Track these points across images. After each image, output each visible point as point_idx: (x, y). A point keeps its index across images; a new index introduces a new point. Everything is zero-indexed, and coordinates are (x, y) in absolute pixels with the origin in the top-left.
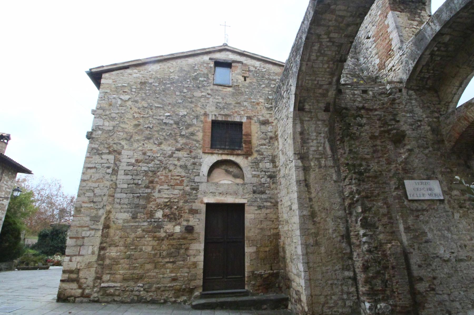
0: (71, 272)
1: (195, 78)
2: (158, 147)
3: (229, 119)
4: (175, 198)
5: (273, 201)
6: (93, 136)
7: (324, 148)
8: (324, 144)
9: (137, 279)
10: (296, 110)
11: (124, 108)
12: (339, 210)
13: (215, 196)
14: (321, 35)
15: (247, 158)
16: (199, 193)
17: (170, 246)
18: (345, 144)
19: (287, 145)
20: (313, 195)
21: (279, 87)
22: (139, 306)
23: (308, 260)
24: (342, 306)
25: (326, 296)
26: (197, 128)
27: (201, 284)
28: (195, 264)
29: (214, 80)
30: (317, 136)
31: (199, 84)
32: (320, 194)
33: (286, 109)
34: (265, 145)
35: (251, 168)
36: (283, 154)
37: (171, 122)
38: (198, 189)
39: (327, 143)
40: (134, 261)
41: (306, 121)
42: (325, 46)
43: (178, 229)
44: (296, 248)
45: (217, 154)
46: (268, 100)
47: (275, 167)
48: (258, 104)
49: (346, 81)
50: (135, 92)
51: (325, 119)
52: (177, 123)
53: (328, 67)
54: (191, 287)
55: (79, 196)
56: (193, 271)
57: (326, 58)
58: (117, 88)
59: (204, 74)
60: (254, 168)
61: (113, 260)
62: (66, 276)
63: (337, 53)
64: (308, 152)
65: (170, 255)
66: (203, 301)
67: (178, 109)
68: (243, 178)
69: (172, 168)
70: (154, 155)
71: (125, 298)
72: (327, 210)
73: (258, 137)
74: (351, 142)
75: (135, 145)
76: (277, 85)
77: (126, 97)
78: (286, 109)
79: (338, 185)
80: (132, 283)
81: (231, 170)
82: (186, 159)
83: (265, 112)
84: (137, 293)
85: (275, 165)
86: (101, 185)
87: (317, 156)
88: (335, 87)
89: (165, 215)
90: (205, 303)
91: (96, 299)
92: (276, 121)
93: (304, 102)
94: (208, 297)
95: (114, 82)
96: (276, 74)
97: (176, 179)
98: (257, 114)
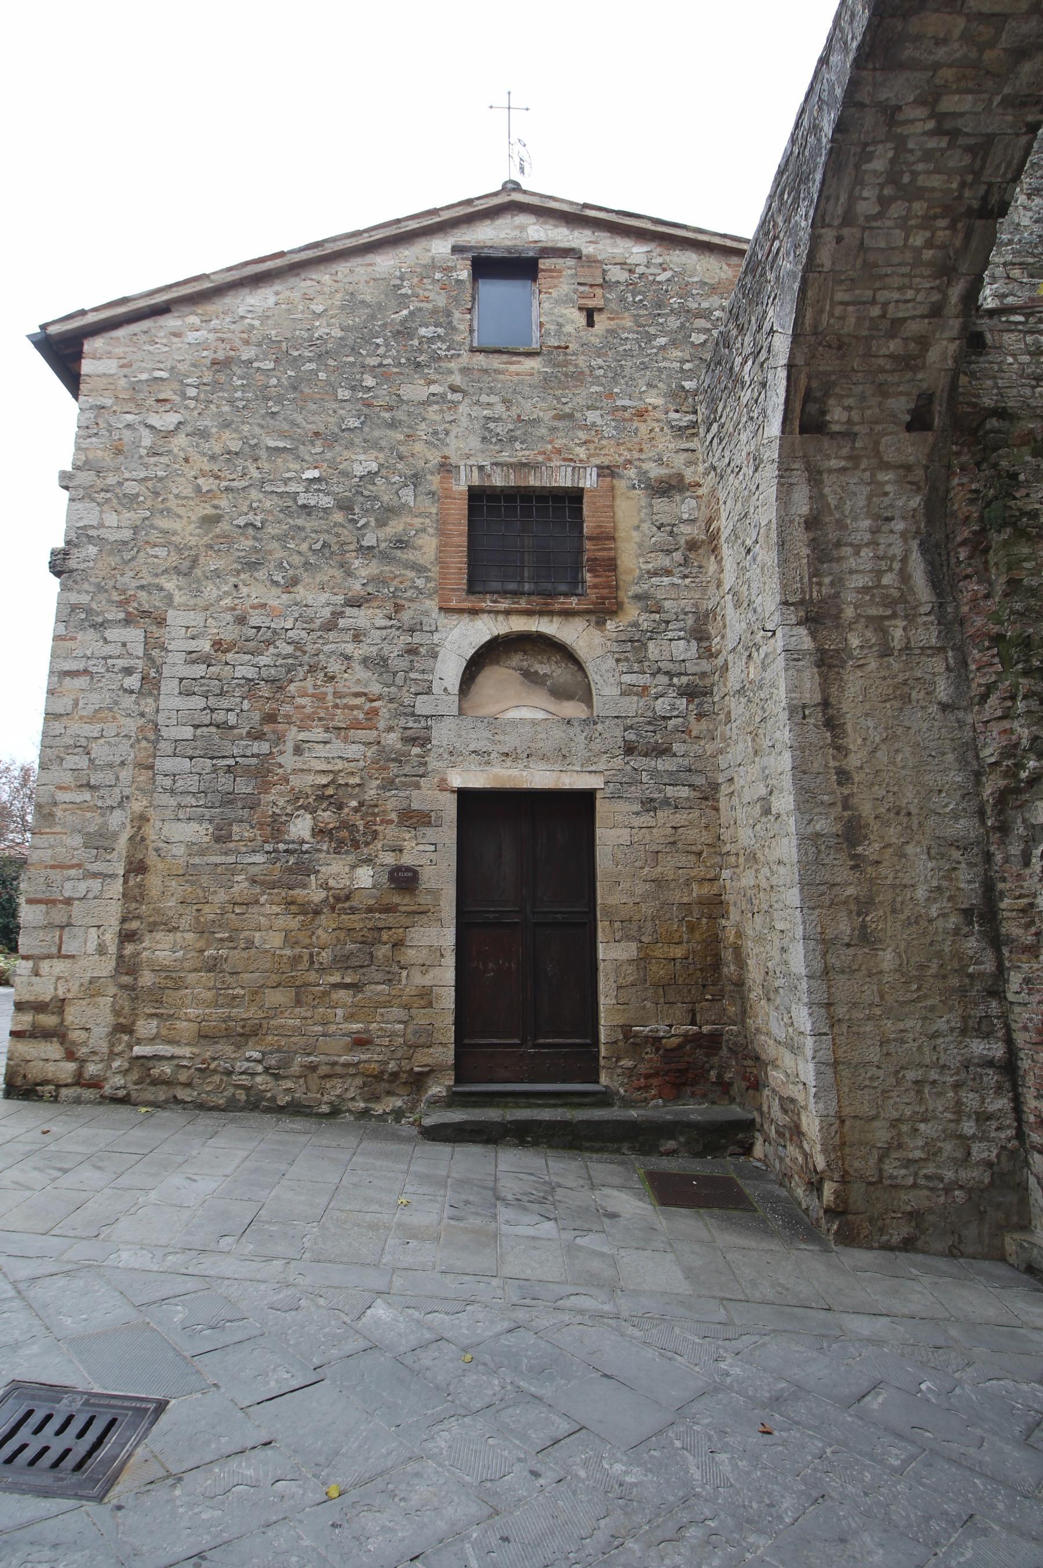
0: (39, 1007)
1: (404, 332)
2: (285, 596)
3: (533, 481)
5: (699, 780)
6: (72, 564)
7: (905, 577)
8: (904, 560)
9: (241, 1035)
10: (791, 433)
11: (164, 460)
12: (955, 816)
13: (488, 763)
14: (899, 108)
15: (600, 624)
16: (432, 754)
18: (992, 558)
19: (754, 573)
20: (854, 761)
21: (725, 341)
22: (254, 1119)
23: (830, 994)
25: (895, 1123)
26: (417, 522)
27: (451, 1060)
28: (426, 996)
29: (471, 331)
30: (875, 531)
31: (421, 351)
32: (882, 756)
33: (752, 427)
34: (668, 573)
35: (618, 660)
36: (737, 605)
37: (326, 501)
38: (429, 740)
39: (916, 557)
40: (229, 979)
41: (830, 471)
42: (919, 154)
43: (364, 877)
44: (784, 950)
45: (489, 612)
46: (678, 396)
47: (709, 654)
48: (641, 414)
49: (1004, 296)
50: (196, 399)
51: (912, 459)
52: (345, 506)
53: (929, 244)
54: (417, 1069)
55: (43, 767)
56: (422, 1018)
57: (919, 207)
58: (134, 388)
59: (434, 312)
60: (627, 659)
61: (164, 975)
62: (27, 1020)
63: (969, 178)
64: (837, 595)
65: (342, 962)
66: (456, 1116)
67: (346, 454)
68: (587, 697)
69: (335, 666)
70: (273, 625)
71: (207, 1093)
72: (909, 814)
73: (640, 545)
74: (1015, 550)
75: (210, 591)
76: (715, 333)
77: (168, 420)
78: (752, 427)
79: (958, 721)
80: (226, 1049)
81: (542, 669)
82: (384, 632)
83: (666, 443)
84: (245, 1080)
85: (708, 649)
86: (111, 730)
87: (873, 611)
88: (954, 325)
89: (321, 831)
90: (466, 1122)
91: (121, 1093)
92: (711, 479)
93: (826, 395)
94: (475, 1105)
95: (121, 367)
96: (714, 289)
97: (352, 708)
98: (636, 455)
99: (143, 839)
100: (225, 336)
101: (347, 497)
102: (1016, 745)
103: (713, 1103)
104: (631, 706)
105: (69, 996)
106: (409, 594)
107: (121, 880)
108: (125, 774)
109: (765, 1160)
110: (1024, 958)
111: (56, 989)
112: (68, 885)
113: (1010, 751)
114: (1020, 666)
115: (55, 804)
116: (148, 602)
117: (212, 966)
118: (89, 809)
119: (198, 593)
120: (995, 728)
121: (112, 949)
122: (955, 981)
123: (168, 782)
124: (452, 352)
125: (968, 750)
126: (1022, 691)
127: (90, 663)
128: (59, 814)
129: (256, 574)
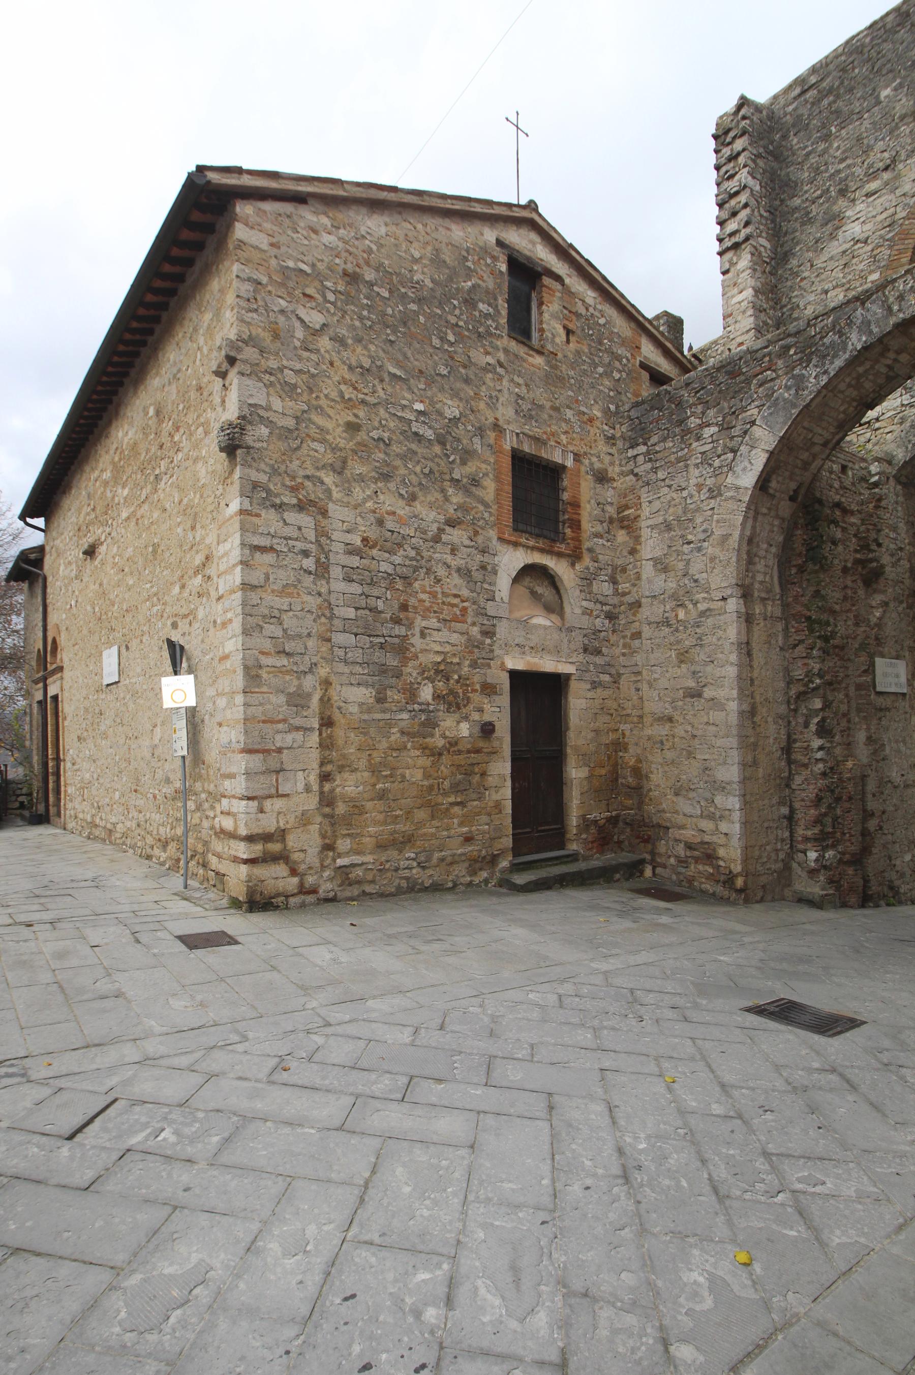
0: (267, 838)
4: (454, 655)
9: (402, 843)
13: (524, 653)
17: (454, 769)
38: (494, 634)
40: (392, 804)
43: (464, 729)
45: (524, 546)
65: (456, 788)
69: (441, 572)
71: (384, 885)
80: (393, 853)
81: (540, 590)
82: (469, 550)
84: (407, 873)
89: (438, 696)
91: (331, 894)
97: (453, 605)
99: (329, 699)
100: (351, 249)
101: (442, 434)
104: (585, 622)
105: (288, 826)
106: (480, 523)
107: (317, 733)
108: (311, 643)
111: (278, 822)
112: (278, 737)
115: (260, 667)
116: (314, 492)
117: (382, 796)
118: (288, 672)
119: (349, 492)
121: (316, 787)
123: (341, 653)
124: (498, 332)
127: (275, 541)
128: (265, 676)
129: (389, 485)
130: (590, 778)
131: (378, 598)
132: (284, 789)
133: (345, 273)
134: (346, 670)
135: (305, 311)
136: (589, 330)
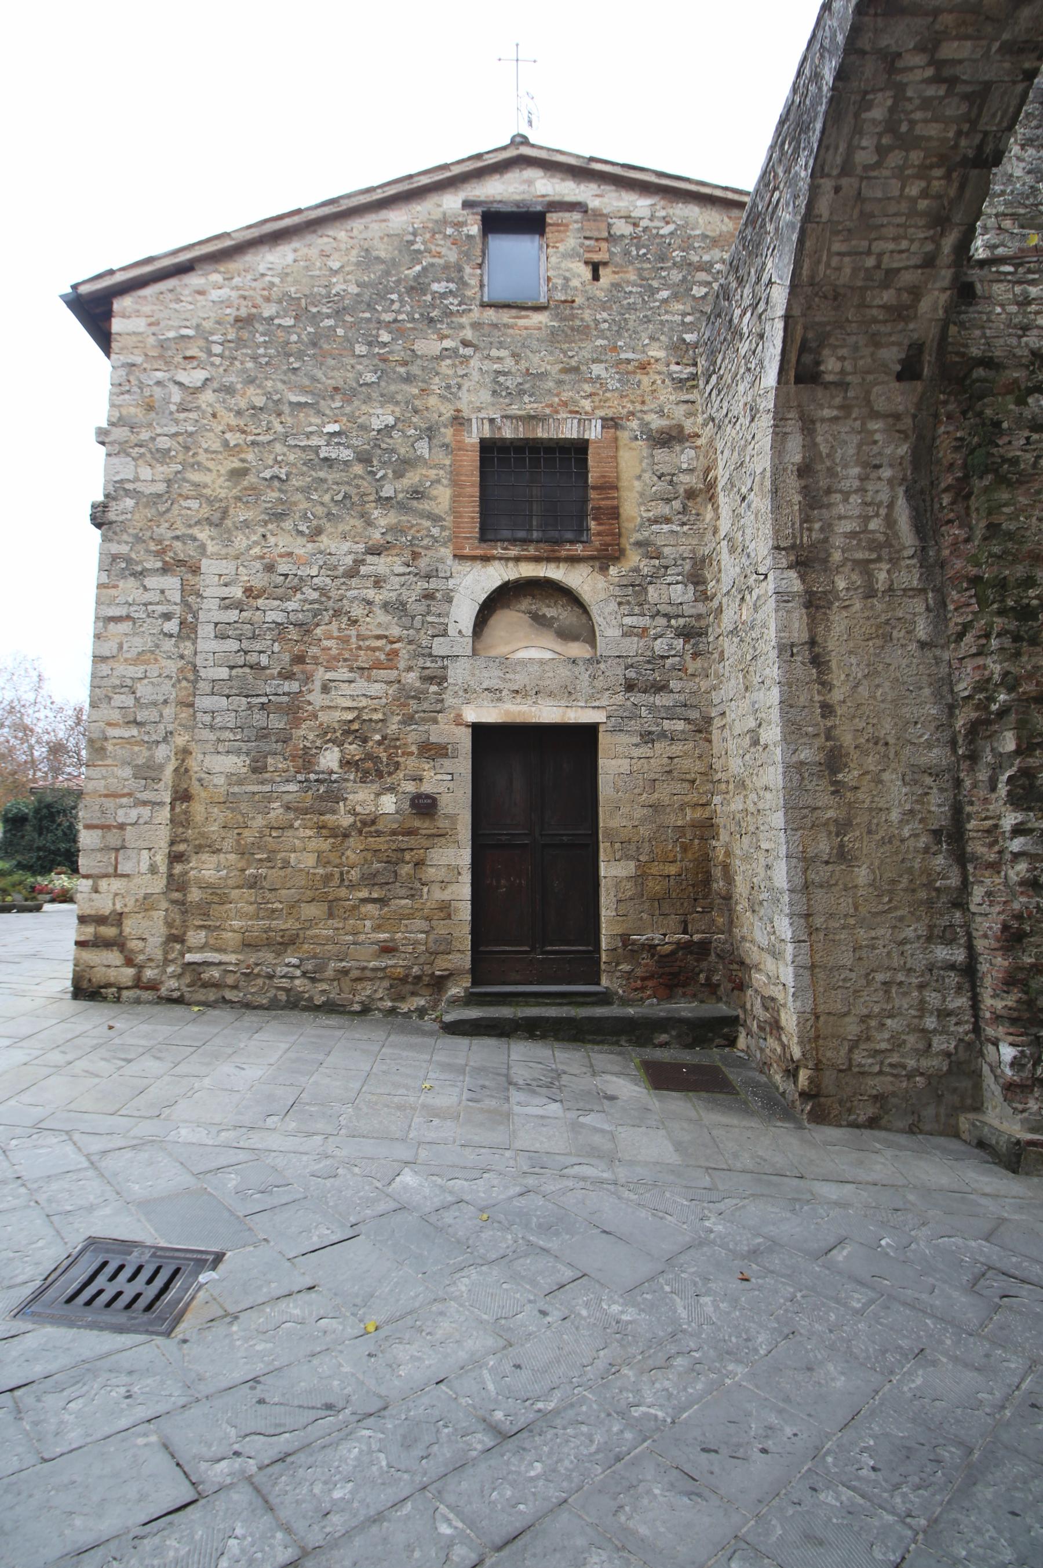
0: (100, 920)
1: (417, 288)
2: (310, 545)
3: (541, 433)
4: (376, 710)
5: (694, 714)
6: (111, 516)
7: (890, 522)
8: (891, 506)
9: (281, 944)
10: (787, 383)
11: (193, 415)
12: (929, 746)
13: (500, 700)
14: (899, 55)
15: (604, 569)
16: (448, 692)
17: (369, 855)
18: (973, 503)
19: (749, 519)
20: (836, 696)
21: (725, 293)
22: (294, 1016)
23: (809, 906)
24: (917, 1050)
26: (432, 473)
27: (467, 964)
28: (445, 909)
29: (482, 286)
30: (864, 478)
31: (433, 306)
32: (864, 691)
33: (749, 378)
34: (668, 521)
35: (620, 604)
36: (732, 550)
37: (346, 454)
38: (445, 679)
39: (901, 502)
41: (823, 420)
42: (917, 102)
43: (388, 804)
44: (768, 867)
45: (500, 559)
46: (680, 349)
47: (704, 597)
48: (643, 367)
49: (996, 246)
50: (221, 356)
51: (901, 408)
52: (364, 459)
53: (924, 194)
54: (438, 973)
55: (93, 705)
56: (441, 929)
57: (916, 157)
58: (162, 345)
59: (446, 267)
60: (628, 603)
61: (210, 891)
62: (90, 930)
63: (966, 127)
64: (826, 540)
65: (370, 880)
66: (473, 1013)
67: (364, 408)
68: (591, 639)
69: (357, 611)
70: (299, 573)
71: (252, 994)
72: (887, 744)
73: (642, 494)
74: (996, 496)
75: (241, 541)
76: (715, 286)
77: (195, 377)
78: (749, 378)
79: (935, 658)
80: (267, 956)
81: (550, 612)
82: (403, 579)
83: (668, 396)
84: (285, 983)
85: (704, 592)
86: (153, 671)
87: (860, 555)
88: (946, 275)
89: (348, 762)
90: (482, 1019)
91: (176, 995)
92: (709, 430)
93: (821, 346)
94: (491, 1004)
95: (150, 325)
96: (715, 242)
97: (374, 649)
98: (639, 407)
99: (187, 771)
100: (246, 293)
101: (366, 450)
102: (989, 680)
103: (702, 1002)
105: (126, 910)
106: (425, 542)
107: (168, 808)
108: (168, 711)
109: (747, 1051)
110: (987, 873)
112: (121, 812)
113: (983, 685)
114: (995, 606)
116: (183, 551)
117: (253, 883)
119: (228, 542)
120: (970, 665)
121: (163, 869)
122: (923, 895)
123: (207, 718)
124: (464, 307)
125: (944, 684)
126: (996, 629)
127: (132, 609)
128: (110, 748)
129: (282, 525)
130: (640, 877)
131: (260, 652)
132: (124, 868)
133: (237, 320)
134: (212, 737)
135: (185, 373)
136: (638, 249)
